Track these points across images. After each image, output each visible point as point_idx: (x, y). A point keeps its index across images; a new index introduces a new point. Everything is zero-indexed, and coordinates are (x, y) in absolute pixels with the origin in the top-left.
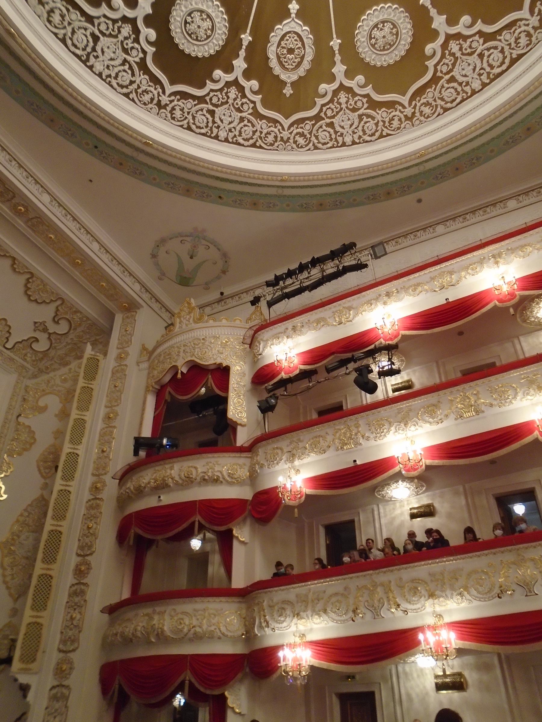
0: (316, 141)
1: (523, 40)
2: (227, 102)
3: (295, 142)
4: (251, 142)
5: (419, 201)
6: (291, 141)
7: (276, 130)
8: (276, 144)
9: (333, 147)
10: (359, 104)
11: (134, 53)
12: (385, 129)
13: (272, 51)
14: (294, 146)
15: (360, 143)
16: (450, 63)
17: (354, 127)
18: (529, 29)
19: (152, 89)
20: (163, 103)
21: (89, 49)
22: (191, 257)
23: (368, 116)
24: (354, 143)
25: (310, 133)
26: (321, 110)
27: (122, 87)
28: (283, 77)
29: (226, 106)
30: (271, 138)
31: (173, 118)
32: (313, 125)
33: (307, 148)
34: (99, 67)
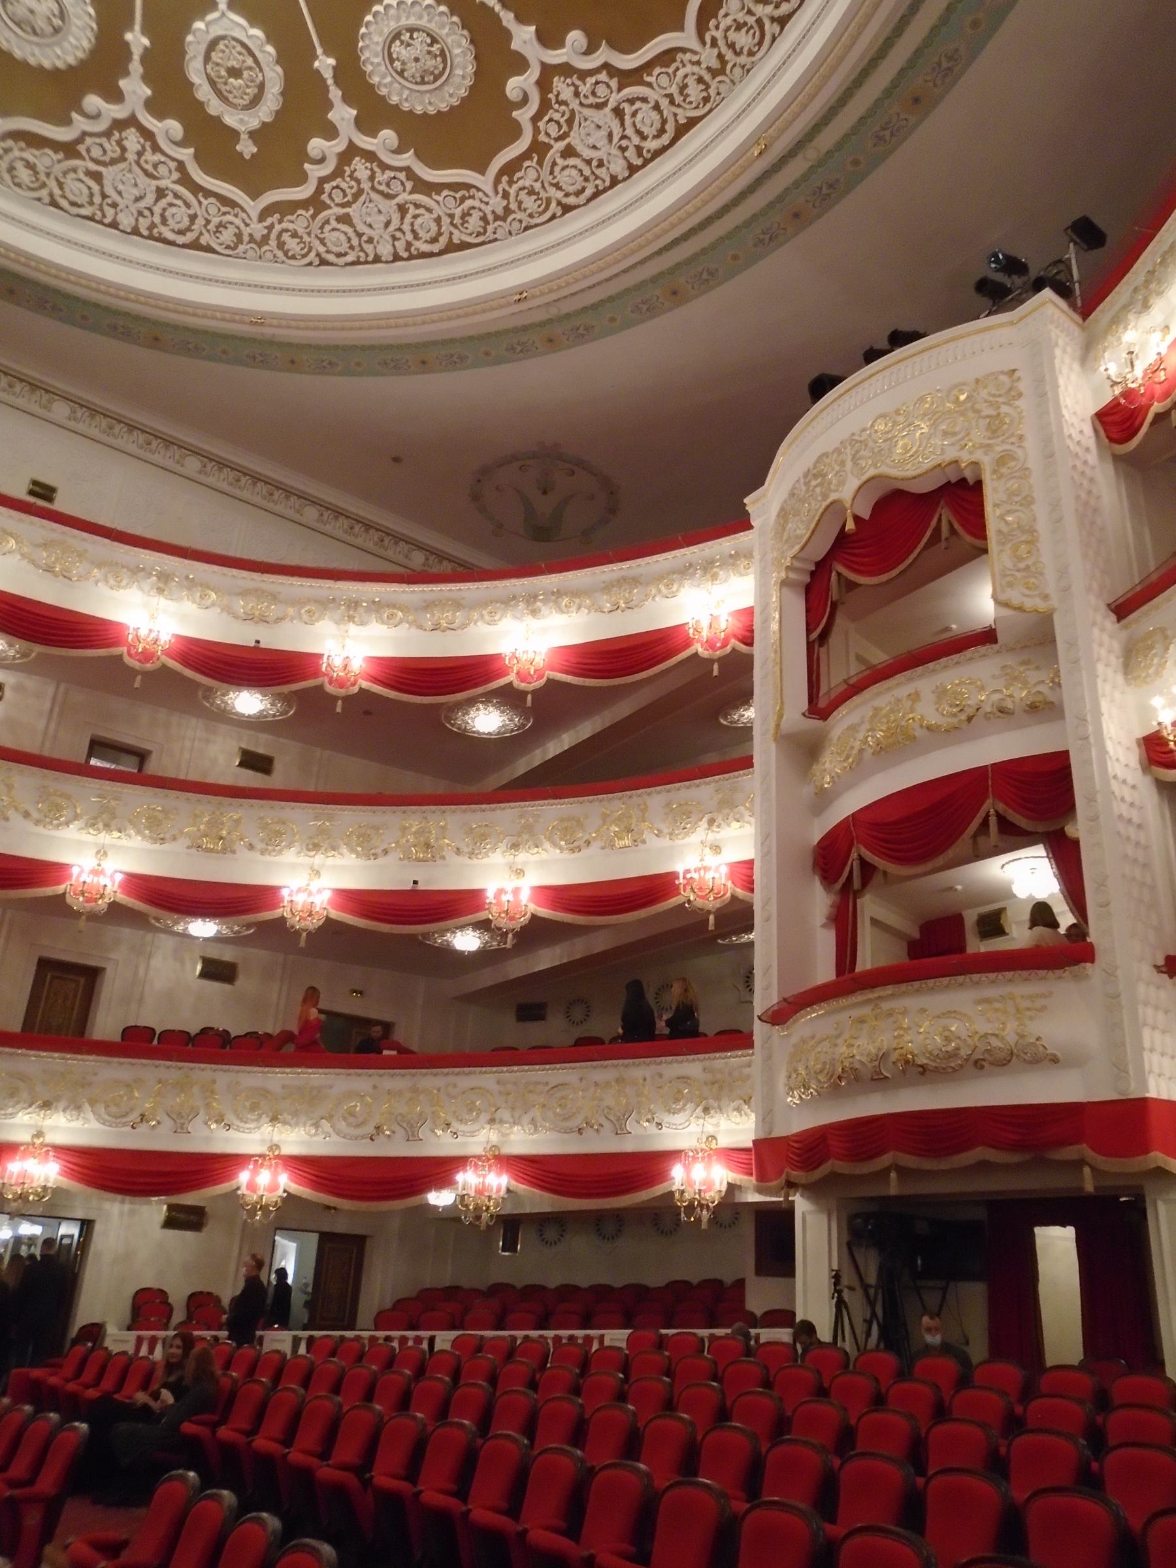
1: (227, 236)
18: (246, 231)
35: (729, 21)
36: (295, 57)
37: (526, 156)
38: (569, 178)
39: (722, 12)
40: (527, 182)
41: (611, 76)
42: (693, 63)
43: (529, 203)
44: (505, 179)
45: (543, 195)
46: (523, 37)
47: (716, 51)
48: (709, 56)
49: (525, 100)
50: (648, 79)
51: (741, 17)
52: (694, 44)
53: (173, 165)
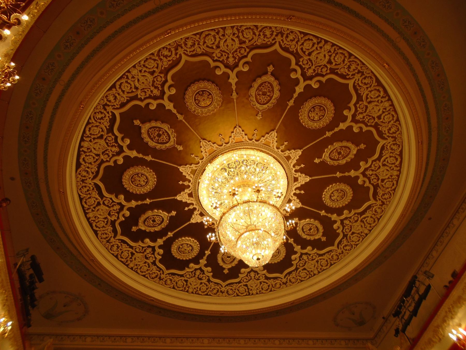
0: (354, 243)
2: (306, 262)
3: (346, 250)
4: (329, 265)
5: (430, 219)
6: (344, 251)
7: (334, 253)
8: (340, 257)
9: (363, 239)
10: (356, 219)
11: (261, 277)
12: (377, 216)
13: (304, 236)
14: (347, 251)
15: (373, 229)
16: (375, 177)
17: (363, 226)
18: (391, 143)
19: (277, 281)
20: (285, 282)
21: (247, 290)
22: (353, 314)
23: (365, 218)
24: (370, 231)
25: (348, 242)
26: (343, 233)
27: (267, 290)
28: (317, 237)
29: (307, 263)
30: (335, 257)
31: (293, 283)
32: (347, 239)
33: (353, 248)
34: (254, 292)
35: (265, 39)
36: (330, 141)
37: (337, 74)
38: (339, 59)
39: (264, 42)
40: (346, 70)
41: (300, 61)
42: (283, 42)
43: (353, 67)
44: (347, 77)
45: (348, 64)
46: (299, 89)
47: (276, 38)
48: (279, 38)
49: (319, 81)
50: (295, 51)
51: (262, 37)
52: (277, 44)
53: (374, 163)
